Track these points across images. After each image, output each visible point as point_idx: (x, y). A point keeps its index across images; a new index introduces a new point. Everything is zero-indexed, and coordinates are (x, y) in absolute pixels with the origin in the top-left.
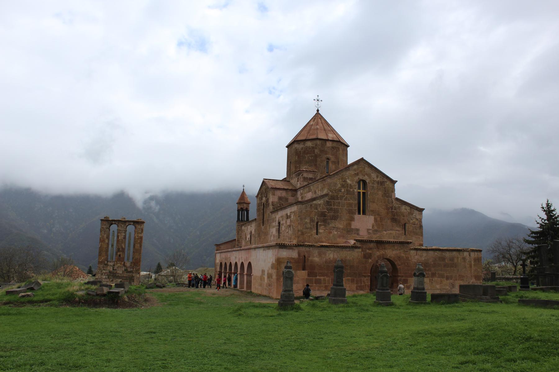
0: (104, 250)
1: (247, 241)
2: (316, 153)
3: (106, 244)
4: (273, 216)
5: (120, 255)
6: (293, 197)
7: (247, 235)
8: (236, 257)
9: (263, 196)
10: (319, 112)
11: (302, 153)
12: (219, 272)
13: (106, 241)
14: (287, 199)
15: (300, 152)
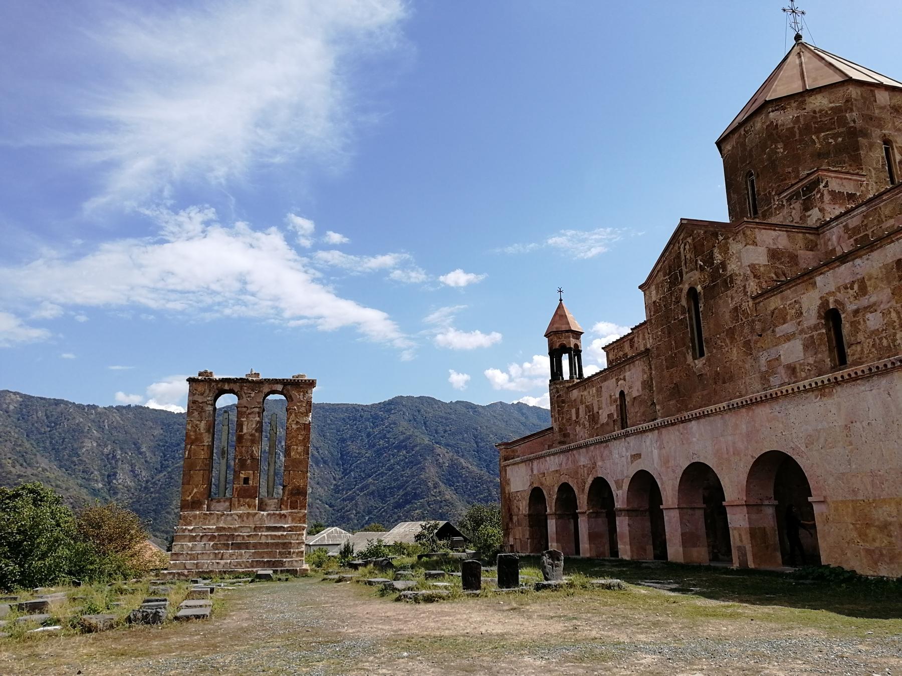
0: (198, 468)
1: (603, 424)
2: (852, 124)
3: (205, 448)
4: (775, 302)
5: (246, 480)
6: (812, 251)
7: (599, 409)
8: (636, 456)
9: (684, 269)
10: (803, 40)
11: (797, 131)
12: (529, 515)
13: (207, 440)
14: (793, 259)
15: (791, 130)
